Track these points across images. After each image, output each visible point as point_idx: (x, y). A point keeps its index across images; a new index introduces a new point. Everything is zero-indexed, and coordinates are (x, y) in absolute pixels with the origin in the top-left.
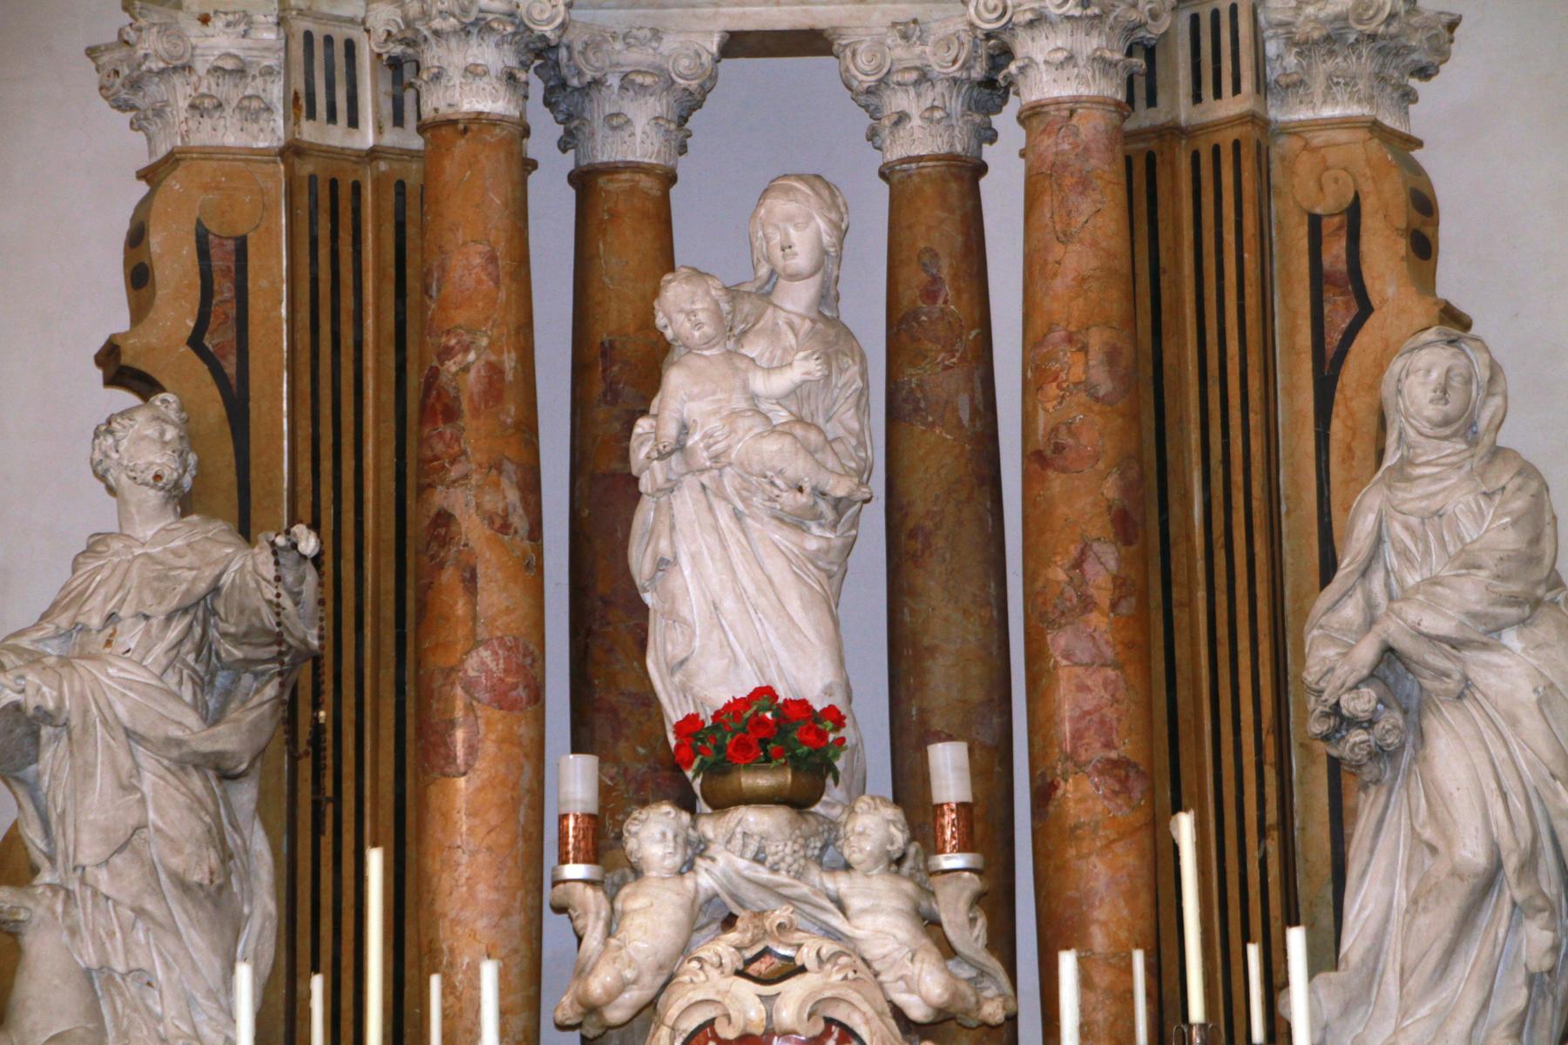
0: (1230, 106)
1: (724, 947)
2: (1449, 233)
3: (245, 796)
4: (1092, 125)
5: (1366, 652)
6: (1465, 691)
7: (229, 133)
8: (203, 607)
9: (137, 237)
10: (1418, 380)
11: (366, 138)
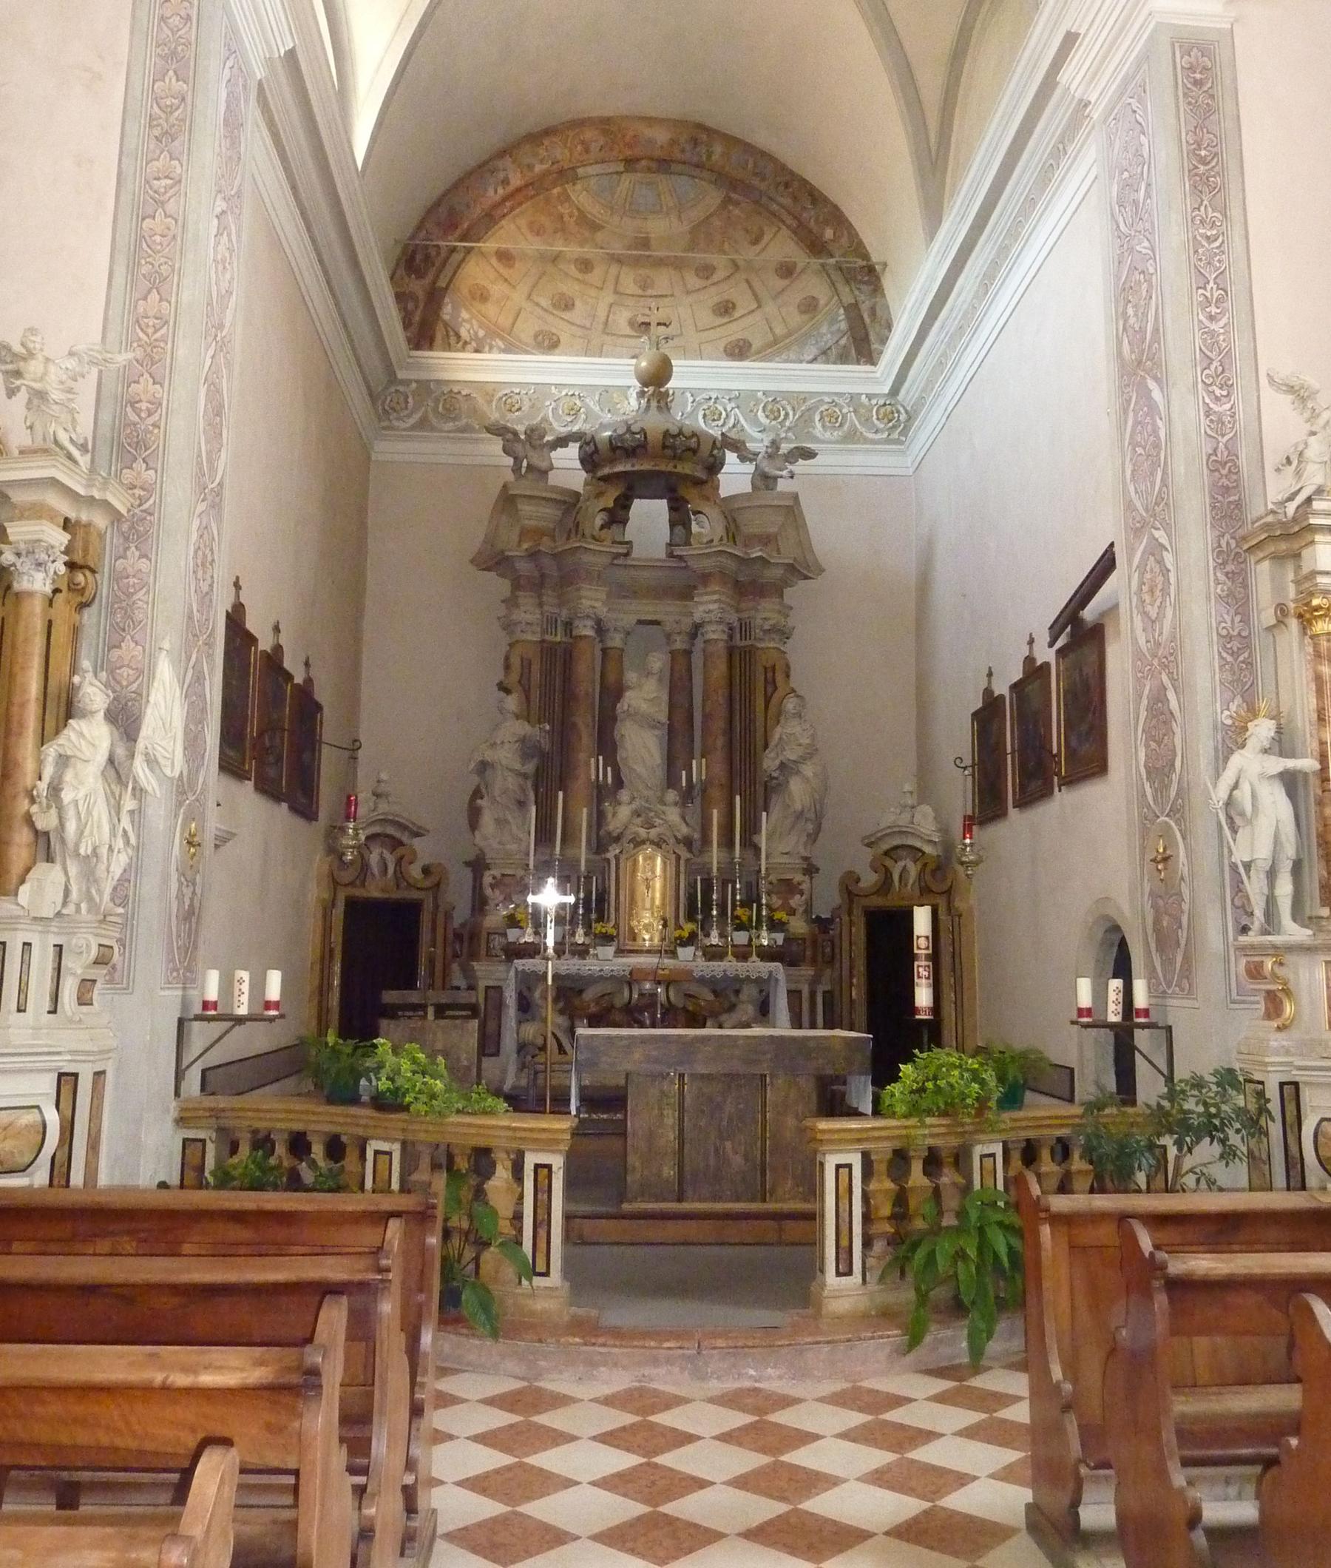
0: (749, 642)
1: (639, 821)
2: (792, 673)
3: (529, 783)
4: (721, 644)
5: (777, 762)
6: (798, 772)
7: (529, 637)
8: (523, 740)
9: (507, 658)
10: (790, 704)
11: (558, 639)
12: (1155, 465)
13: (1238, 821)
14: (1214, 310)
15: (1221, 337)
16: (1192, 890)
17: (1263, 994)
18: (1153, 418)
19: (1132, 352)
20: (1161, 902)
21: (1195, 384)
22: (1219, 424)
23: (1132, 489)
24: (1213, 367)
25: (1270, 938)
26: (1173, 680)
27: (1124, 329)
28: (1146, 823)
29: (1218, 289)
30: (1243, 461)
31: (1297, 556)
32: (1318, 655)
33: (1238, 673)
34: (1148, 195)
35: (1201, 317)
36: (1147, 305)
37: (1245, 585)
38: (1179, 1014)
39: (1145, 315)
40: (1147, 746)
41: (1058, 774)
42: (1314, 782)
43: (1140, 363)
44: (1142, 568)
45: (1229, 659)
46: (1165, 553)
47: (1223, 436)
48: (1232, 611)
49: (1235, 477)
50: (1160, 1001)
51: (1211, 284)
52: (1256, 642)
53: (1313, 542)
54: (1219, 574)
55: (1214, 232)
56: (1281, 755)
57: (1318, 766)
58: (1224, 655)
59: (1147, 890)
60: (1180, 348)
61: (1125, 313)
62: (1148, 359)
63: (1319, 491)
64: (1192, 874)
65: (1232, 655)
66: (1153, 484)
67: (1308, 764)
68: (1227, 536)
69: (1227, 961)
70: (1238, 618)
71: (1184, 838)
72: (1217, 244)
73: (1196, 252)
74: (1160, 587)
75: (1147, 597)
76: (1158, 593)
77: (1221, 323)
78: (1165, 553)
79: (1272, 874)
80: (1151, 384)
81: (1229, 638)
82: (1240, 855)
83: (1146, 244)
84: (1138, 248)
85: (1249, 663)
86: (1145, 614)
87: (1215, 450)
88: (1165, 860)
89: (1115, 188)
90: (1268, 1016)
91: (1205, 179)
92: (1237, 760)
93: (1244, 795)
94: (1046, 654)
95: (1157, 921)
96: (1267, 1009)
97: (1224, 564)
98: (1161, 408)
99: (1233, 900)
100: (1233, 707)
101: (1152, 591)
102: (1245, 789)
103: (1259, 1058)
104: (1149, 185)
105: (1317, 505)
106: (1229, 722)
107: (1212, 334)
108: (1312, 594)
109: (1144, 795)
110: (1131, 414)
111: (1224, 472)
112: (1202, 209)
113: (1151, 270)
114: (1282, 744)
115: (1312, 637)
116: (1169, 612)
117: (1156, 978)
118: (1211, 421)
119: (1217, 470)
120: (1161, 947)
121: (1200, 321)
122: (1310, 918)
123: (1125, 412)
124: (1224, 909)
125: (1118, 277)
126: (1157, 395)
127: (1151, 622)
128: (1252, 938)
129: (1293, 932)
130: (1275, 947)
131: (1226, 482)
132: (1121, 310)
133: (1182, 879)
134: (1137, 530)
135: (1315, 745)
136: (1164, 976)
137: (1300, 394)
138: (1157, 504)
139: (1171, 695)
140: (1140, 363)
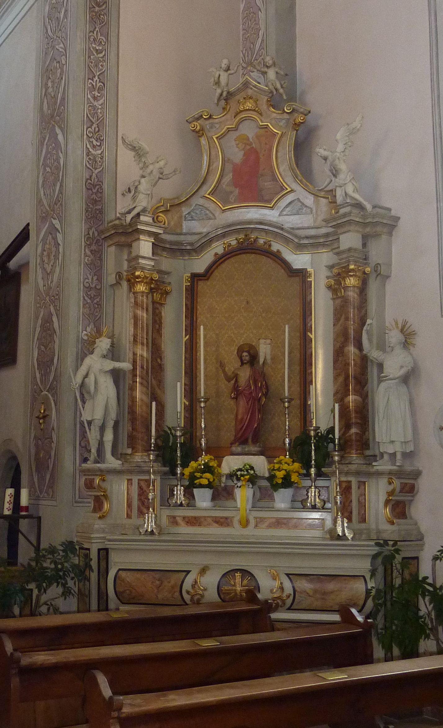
13: (86, 396)
14: (97, 94)
15: (99, 111)
17: (93, 497)
21: (82, 135)
22: (93, 162)
25: (98, 465)
26: (56, 310)
27: (45, 94)
28: (36, 397)
29: (100, 82)
30: (105, 186)
31: (130, 246)
32: (136, 303)
33: (93, 310)
34: (65, 16)
35: (89, 96)
37: (101, 259)
38: (46, 510)
40: (39, 349)
42: (129, 376)
43: (52, 116)
45: (89, 301)
46: (58, 234)
47: (96, 169)
49: (99, 195)
51: (97, 77)
53: (139, 239)
55: (100, 48)
56: (112, 360)
57: (131, 367)
58: (86, 298)
59: (33, 435)
60: (76, 111)
62: (57, 115)
63: (144, 210)
64: (59, 428)
66: (54, 191)
67: (126, 366)
68: (93, 229)
69: (74, 477)
70: (95, 278)
71: (55, 405)
72: (101, 55)
73: (89, 57)
74: (53, 254)
75: (46, 259)
76: (52, 257)
77: (101, 101)
78: (58, 234)
79: (102, 429)
80: (58, 131)
81: (90, 288)
82: (86, 416)
83: (62, 45)
84: (57, 47)
85: (99, 305)
86: (44, 269)
88: (44, 417)
89: (47, 8)
90: (95, 511)
91: (98, 15)
92: (88, 361)
93: (90, 381)
97: (90, 245)
98: (63, 146)
99: (80, 444)
100: (89, 329)
101: (49, 256)
102: (92, 378)
104: (66, 11)
105: (142, 218)
107: (94, 107)
108: (135, 269)
110: (45, 146)
111: (94, 191)
112: (95, 32)
113: (64, 62)
114: (114, 353)
115: (134, 293)
116: (58, 269)
118: (90, 159)
120: (38, 470)
122: (121, 454)
123: (42, 144)
124: (75, 447)
126: (60, 137)
127: (47, 274)
129: (112, 462)
130: (101, 470)
131: (94, 196)
132: (44, 83)
133: (53, 429)
134: (43, 218)
135: (131, 355)
137: (138, 152)
138: (56, 204)
139: (55, 319)
140: (52, 116)
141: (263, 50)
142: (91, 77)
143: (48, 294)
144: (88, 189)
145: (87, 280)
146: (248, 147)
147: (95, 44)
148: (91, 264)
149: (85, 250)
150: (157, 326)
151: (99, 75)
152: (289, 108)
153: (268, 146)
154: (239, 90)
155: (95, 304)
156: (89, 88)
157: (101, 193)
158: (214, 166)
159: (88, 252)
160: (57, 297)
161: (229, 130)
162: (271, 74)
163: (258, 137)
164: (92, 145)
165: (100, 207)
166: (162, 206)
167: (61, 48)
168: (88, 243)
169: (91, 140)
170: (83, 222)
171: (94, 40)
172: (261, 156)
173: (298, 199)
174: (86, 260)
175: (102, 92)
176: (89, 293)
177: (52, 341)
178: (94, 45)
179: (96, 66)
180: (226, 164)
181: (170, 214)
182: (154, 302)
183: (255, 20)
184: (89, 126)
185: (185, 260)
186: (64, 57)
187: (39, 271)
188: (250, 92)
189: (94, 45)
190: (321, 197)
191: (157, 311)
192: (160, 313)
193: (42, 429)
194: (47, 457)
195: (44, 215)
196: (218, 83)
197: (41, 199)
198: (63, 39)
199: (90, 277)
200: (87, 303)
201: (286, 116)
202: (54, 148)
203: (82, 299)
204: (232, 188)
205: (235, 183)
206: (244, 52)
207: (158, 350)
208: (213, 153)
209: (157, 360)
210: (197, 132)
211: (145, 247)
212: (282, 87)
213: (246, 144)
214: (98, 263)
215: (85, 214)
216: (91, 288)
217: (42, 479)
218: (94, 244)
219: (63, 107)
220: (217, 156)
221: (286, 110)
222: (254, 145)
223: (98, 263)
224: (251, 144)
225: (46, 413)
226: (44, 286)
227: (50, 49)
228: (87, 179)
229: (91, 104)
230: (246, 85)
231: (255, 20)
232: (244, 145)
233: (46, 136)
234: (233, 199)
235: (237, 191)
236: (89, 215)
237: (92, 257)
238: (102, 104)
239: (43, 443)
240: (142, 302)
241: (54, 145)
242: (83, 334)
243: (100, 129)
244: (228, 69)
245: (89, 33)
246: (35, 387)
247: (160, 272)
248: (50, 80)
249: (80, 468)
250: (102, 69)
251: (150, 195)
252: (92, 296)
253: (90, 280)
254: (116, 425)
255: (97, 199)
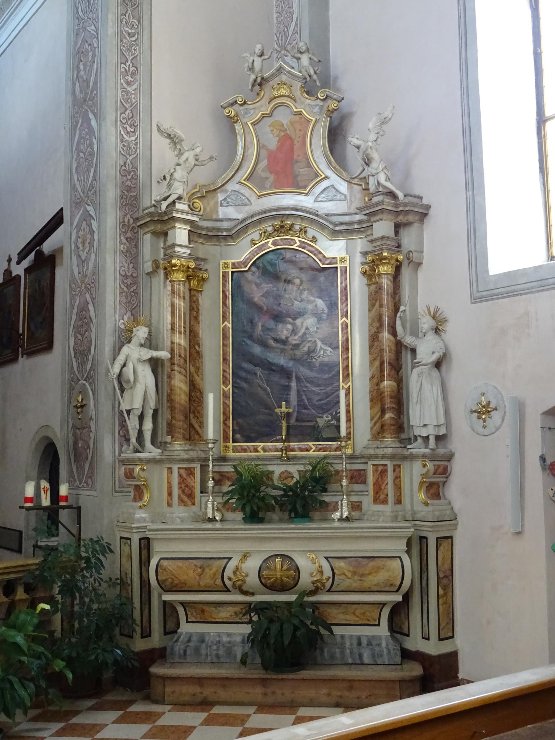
12: (90, 165)
13: (125, 385)
14: (130, 79)
15: (133, 96)
16: (96, 425)
17: (133, 487)
18: (90, 137)
19: (81, 92)
20: (78, 431)
21: (116, 121)
22: (128, 149)
23: (75, 177)
24: (127, 113)
25: (138, 455)
26: (93, 299)
27: (77, 77)
28: (72, 385)
29: (133, 66)
30: (140, 173)
31: (166, 234)
32: (173, 292)
33: (129, 298)
35: (122, 81)
36: (92, 66)
37: (136, 246)
39: (90, 71)
40: (76, 337)
41: (22, 346)
42: (167, 364)
43: (85, 101)
44: (79, 227)
45: (125, 289)
46: (92, 221)
47: (130, 155)
48: (128, 261)
49: (134, 181)
50: (74, 492)
52: (140, 280)
53: (174, 227)
54: (122, 238)
55: (133, 31)
56: (151, 349)
57: (169, 356)
58: (123, 286)
59: (71, 425)
61: (78, 67)
62: (89, 100)
63: (180, 198)
65: (127, 287)
66: (88, 177)
67: (164, 354)
68: (128, 216)
69: (114, 468)
71: (94, 395)
73: (122, 41)
74: (88, 241)
75: (80, 246)
77: (134, 87)
78: (92, 221)
79: (141, 418)
80: (91, 116)
81: (126, 277)
82: (125, 407)
83: (93, 28)
84: (88, 28)
85: (136, 293)
86: (79, 256)
87: (125, 163)
88: (82, 406)
90: (135, 500)
92: (126, 350)
93: (129, 371)
94: (18, 270)
95: (75, 443)
96: (135, 495)
97: (125, 232)
99: (119, 434)
100: (126, 318)
101: (83, 242)
102: (130, 366)
103: (128, 525)
105: (178, 206)
106: (123, 327)
107: (128, 93)
108: (172, 257)
109: (72, 366)
111: (129, 177)
112: (127, 15)
113: (95, 45)
114: (150, 343)
115: (170, 281)
116: (93, 257)
117: (73, 478)
119: (126, 176)
121: (121, 84)
122: (161, 443)
123: (75, 128)
124: (114, 437)
125: (75, 44)
126: (93, 123)
127: (83, 262)
128: (129, 454)
129: (152, 452)
130: (140, 460)
131: (129, 183)
132: (75, 66)
133: (91, 418)
134: (77, 204)
135: (169, 343)
136: (78, 477)
137: (173, 140)
139: (91, 307)
140: (85, 101)
141: (296, 34)
142: (123, 62)
143: (82, 283)
144: (122, 176)
145: (123, 269)
146: (283, 134)
147: (127, 27)
148: (127, 251)
149: (120, 238)
150: (195, 313)
151: (132, 59)
152: (322, 95)
153: (302, 133)
154: (273, 76)
155: (133, 292)
156: (122, 73)
157: (136, 179)
158: (250, 151)
159: (124, 240)
160: (93, 285)
161: (264, 116)
162: (305, 59)
163: (292, 123)
164: (126, 131)
165: (135, 194)
166: (198, 192)
167: (92, 30)
168: (124, 230)
169: (125, 126)
170: (118, 209)
171: (127, 23)
172: (295, 142)
173: (333, 185)
174: (122, 248)
175: (136, 77)
176: (125, 281)
177: (89, 330)
178: (126, 29)
179: (129, 50)
180: (261, 150)
181: (205, 200)
182: (190, 290)
183: (289, 4)
184: (122, 111)
185: (221, 246)
186: (95, 39)
187: (74, 259)
188: (284, 78)
189: (126, 29)
190: (355, 184)
191: (195, 298)
192: (198, 300)
193: (80, 419)
194: (86, 447)
195: (78, 201)
196: (252, 69)
197: (75, 185)
198: (94, 21)
199: (126, 265)
200: (124, 291)
201: (319, 103)
202: (87, 134)
203: (118, 287)
204: (268, 174)
205: (270, 169)
206: (278, 35)
207: (195, 337)
208: (248, 139)
209: (195, 347)
210: (231, 118)
211: (180, 235)
212: (316, 73)
213: (280, 130)
214: (133, 251)
215: (120, 202)
216: (127, 276)
217: (80, 468)
218: (129, 231)
219: (95, 92)
220: (252, 142)
221: (319, 95)
222: (288, 132)
223: (133, 251)
224: (285, 131)
225: (84, 402)
226: (79, 273)
227: (81, 31)
228: (122, 166)
229: (125, 90)
230: (280, 70)
231: (289, 4)
232: (278, 131)
233: (78, 120)
234: (269, 185)
235: (272, 177)
236: (123, 202)
237: (128, 244)
238: (135, 89)
239: (81, 433)
240: (179, 290)
241: (87, 130)
242: (120, 323)
243: (135, 114)
244: (262, 55)
245: (121, 16)
246: (72, 375)
247: (197, 259)
248: (81, 63)
249: (120, 458)
250: (135, 54)
251: (186, 182)
252: (129, 283)
253: (126, 269)
254: (155, 412)
255: (132, 186)
